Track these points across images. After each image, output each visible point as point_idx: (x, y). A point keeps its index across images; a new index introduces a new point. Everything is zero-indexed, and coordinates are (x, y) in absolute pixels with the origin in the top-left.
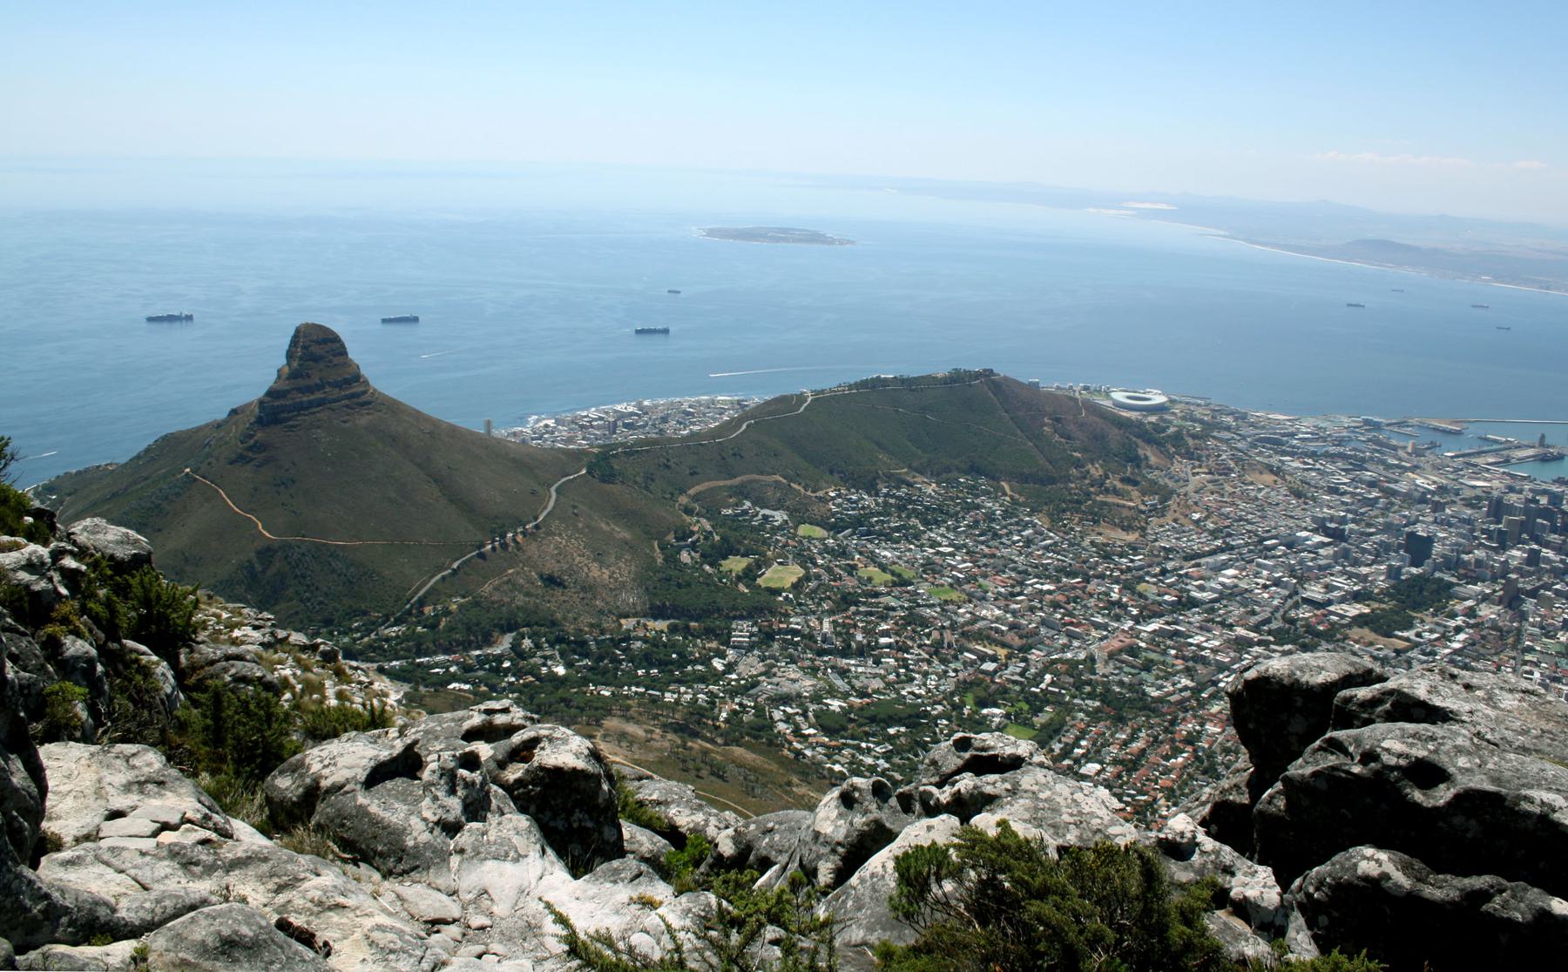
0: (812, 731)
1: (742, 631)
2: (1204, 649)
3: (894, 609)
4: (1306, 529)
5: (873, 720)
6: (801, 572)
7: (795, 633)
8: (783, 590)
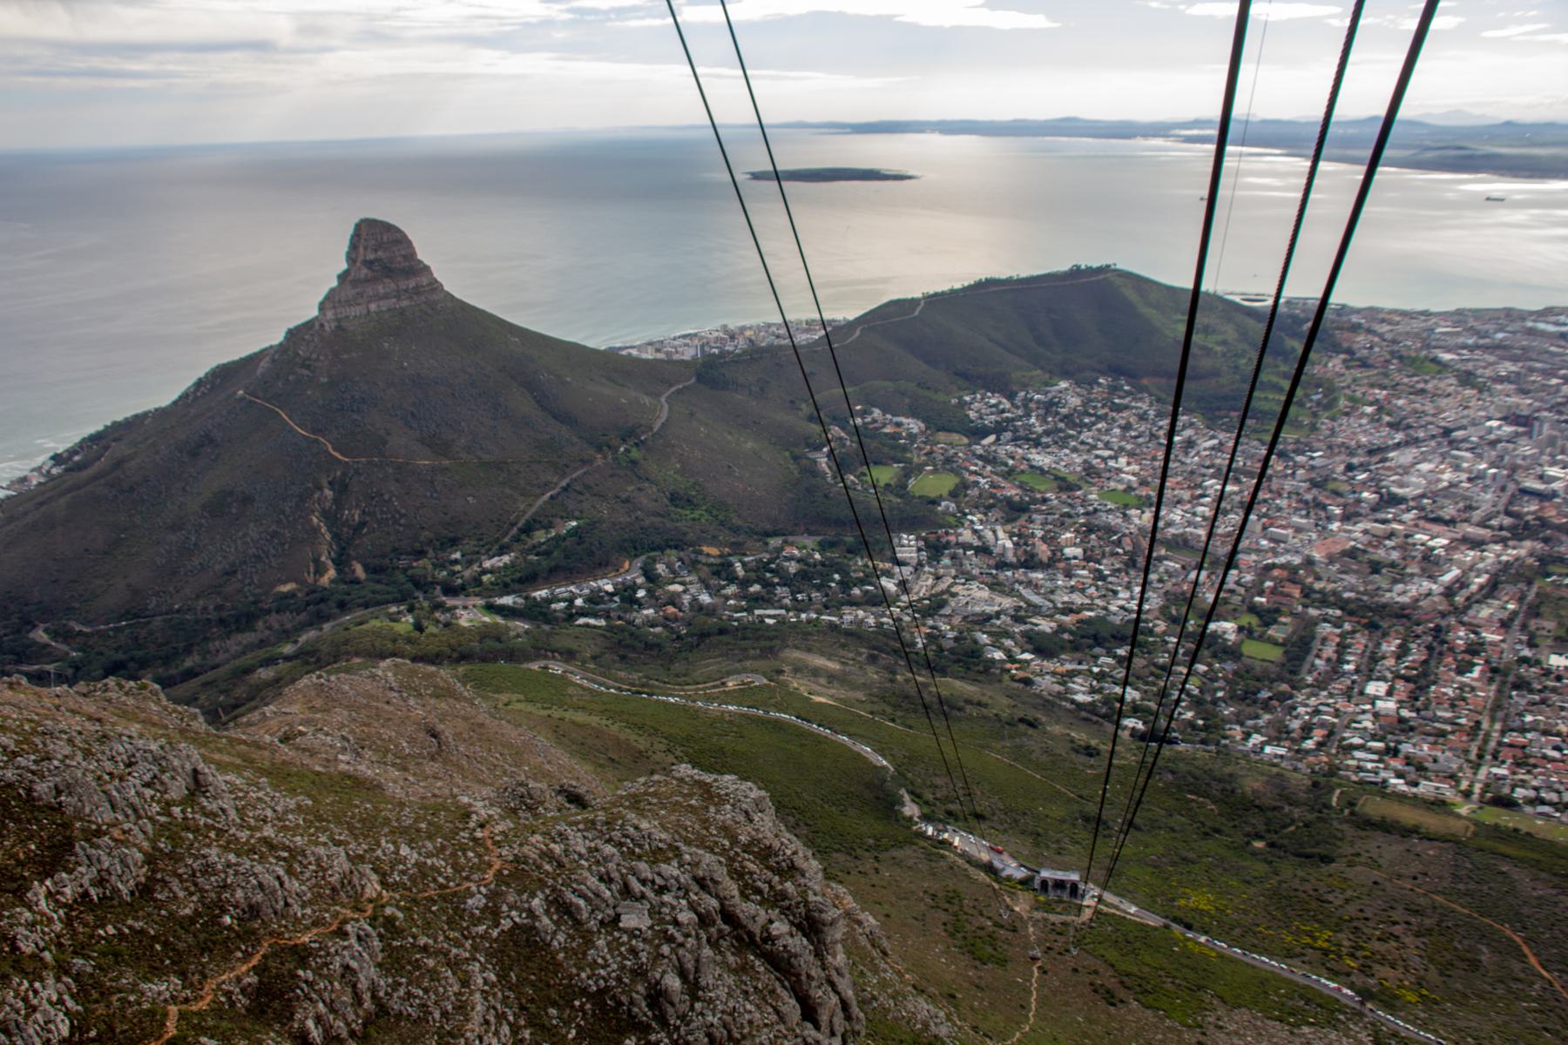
0: (1027, 656)
1: (908, 546)
2: (1433, 549)
3: (1069, 515)
4: (1490, 419)
5: (1098, 640)
6: (957, 480)
7: (966, 546)
8: (941, 498)
